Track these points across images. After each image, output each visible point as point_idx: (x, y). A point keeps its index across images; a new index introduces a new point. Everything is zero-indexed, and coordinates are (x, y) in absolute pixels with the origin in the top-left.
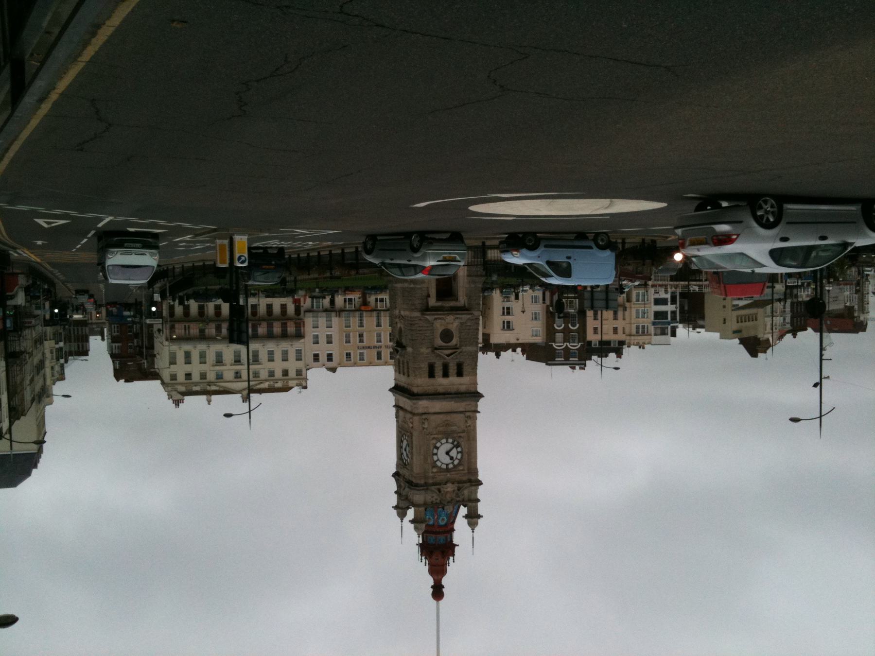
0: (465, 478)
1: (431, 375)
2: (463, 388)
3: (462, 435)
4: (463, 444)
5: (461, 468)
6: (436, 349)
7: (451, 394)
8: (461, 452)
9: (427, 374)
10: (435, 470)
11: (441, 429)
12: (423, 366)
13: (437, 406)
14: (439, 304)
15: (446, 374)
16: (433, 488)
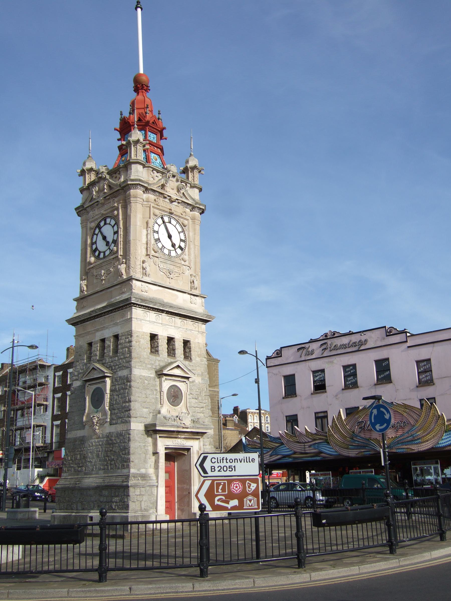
0: (151, 196)
1: (186, 343)
2: (152, 315)
3: (153, 253)
4: (153, 242)
5: (157, 212)
6: (188, 378)
7: (168, 313)
8: (154, 231)
9: (193, 345)
10: (186, 222)
11: (176, 270)
12: (198, 359)
13: (182, 301)
14: (187, 443)
15: (170, 340)
16: (190, 202)
